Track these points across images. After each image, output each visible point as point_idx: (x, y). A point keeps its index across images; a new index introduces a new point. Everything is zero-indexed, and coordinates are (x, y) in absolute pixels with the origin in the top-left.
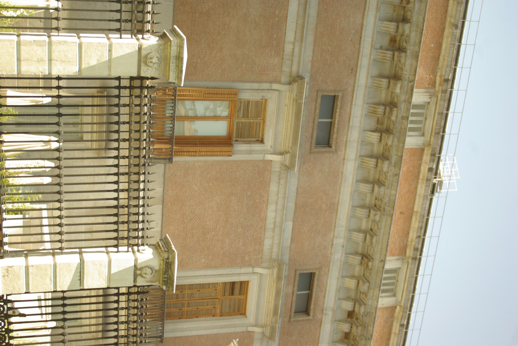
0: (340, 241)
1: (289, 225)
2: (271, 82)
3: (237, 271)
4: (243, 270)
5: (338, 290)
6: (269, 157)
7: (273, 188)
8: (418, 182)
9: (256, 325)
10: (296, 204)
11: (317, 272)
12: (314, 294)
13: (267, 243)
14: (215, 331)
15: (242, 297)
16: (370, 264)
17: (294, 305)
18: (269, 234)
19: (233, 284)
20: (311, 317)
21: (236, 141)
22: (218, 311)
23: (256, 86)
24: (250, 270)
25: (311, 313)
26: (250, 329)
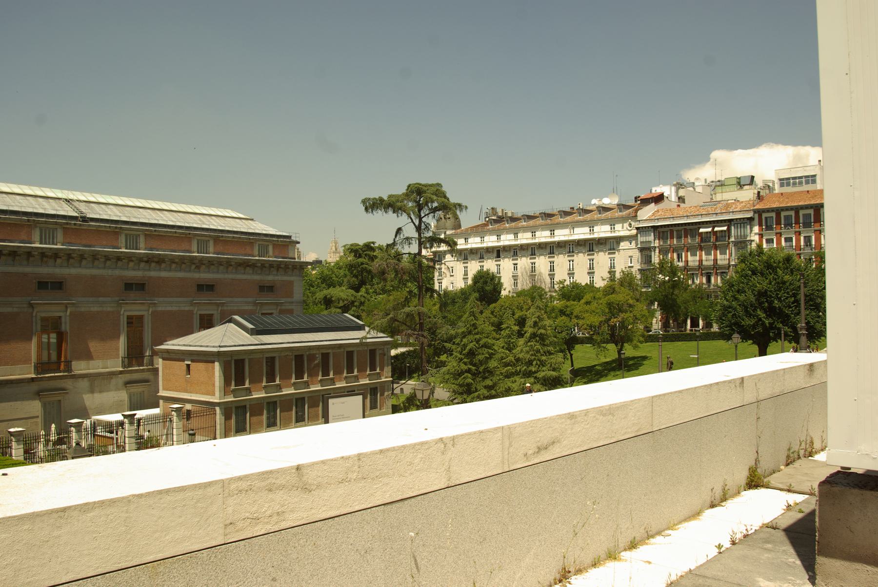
0: (110, 272)
1: (101, 299)
2: (32, 317)
3: (122, 323)
4: (122, 320)
5: (134, 270)
6: (68, 313)
7: (83, 309)
8: (82, 229)
9: (148, 311)
10: (91, 297)
11: (125, 282)
12: (136, 282)
13: (109, 309)
14: (150, 330)
15: (134, 318)
16: (122, 258)
17: (140, 292)
18: (105, 309)
19: (128, 323)
20: (147, 283)
21: (60, 329)
22: (140, 328)
23: (34, 324)
24: (122, 317)
25: (144, 282)
26: (150, 313)
